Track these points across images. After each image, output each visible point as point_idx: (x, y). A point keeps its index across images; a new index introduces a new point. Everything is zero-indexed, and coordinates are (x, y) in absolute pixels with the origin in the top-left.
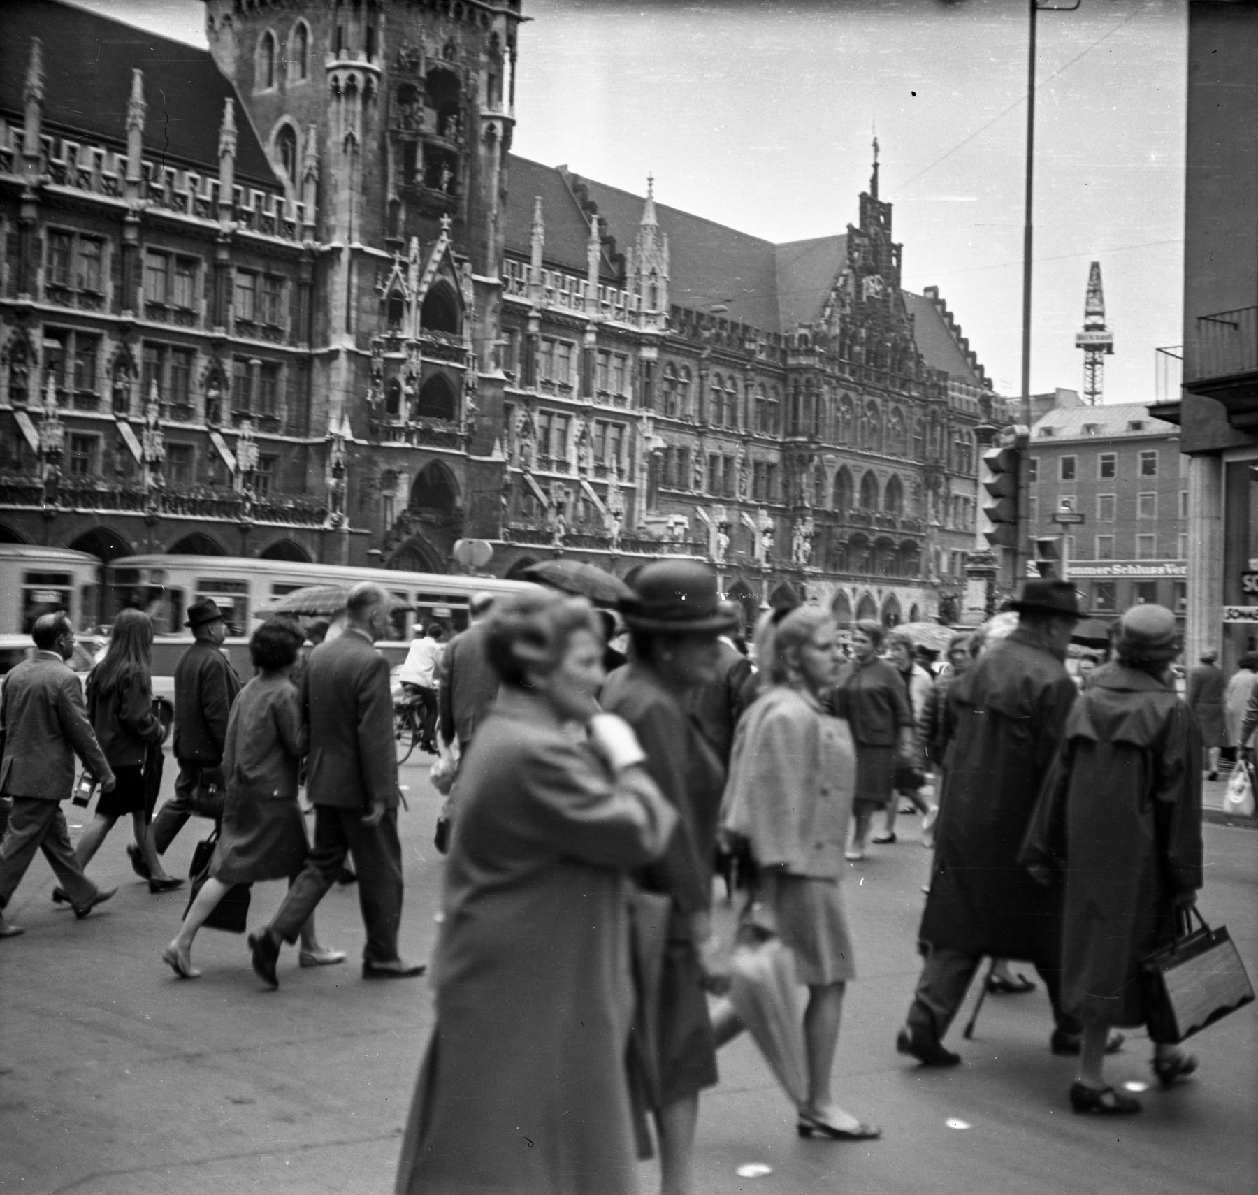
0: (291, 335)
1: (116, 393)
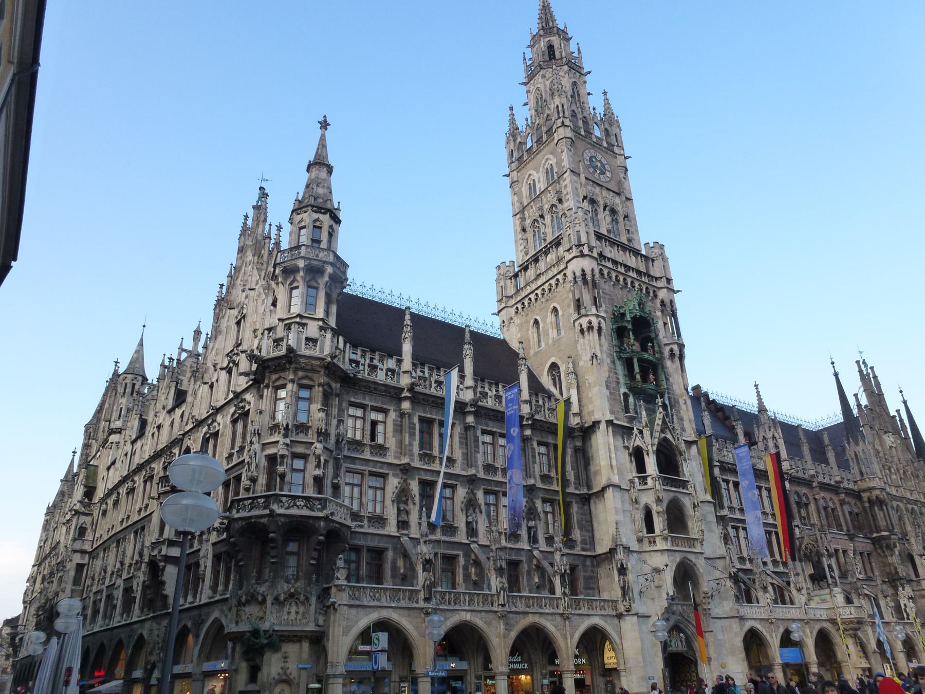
0: (575, 483)
1: (468, 524)
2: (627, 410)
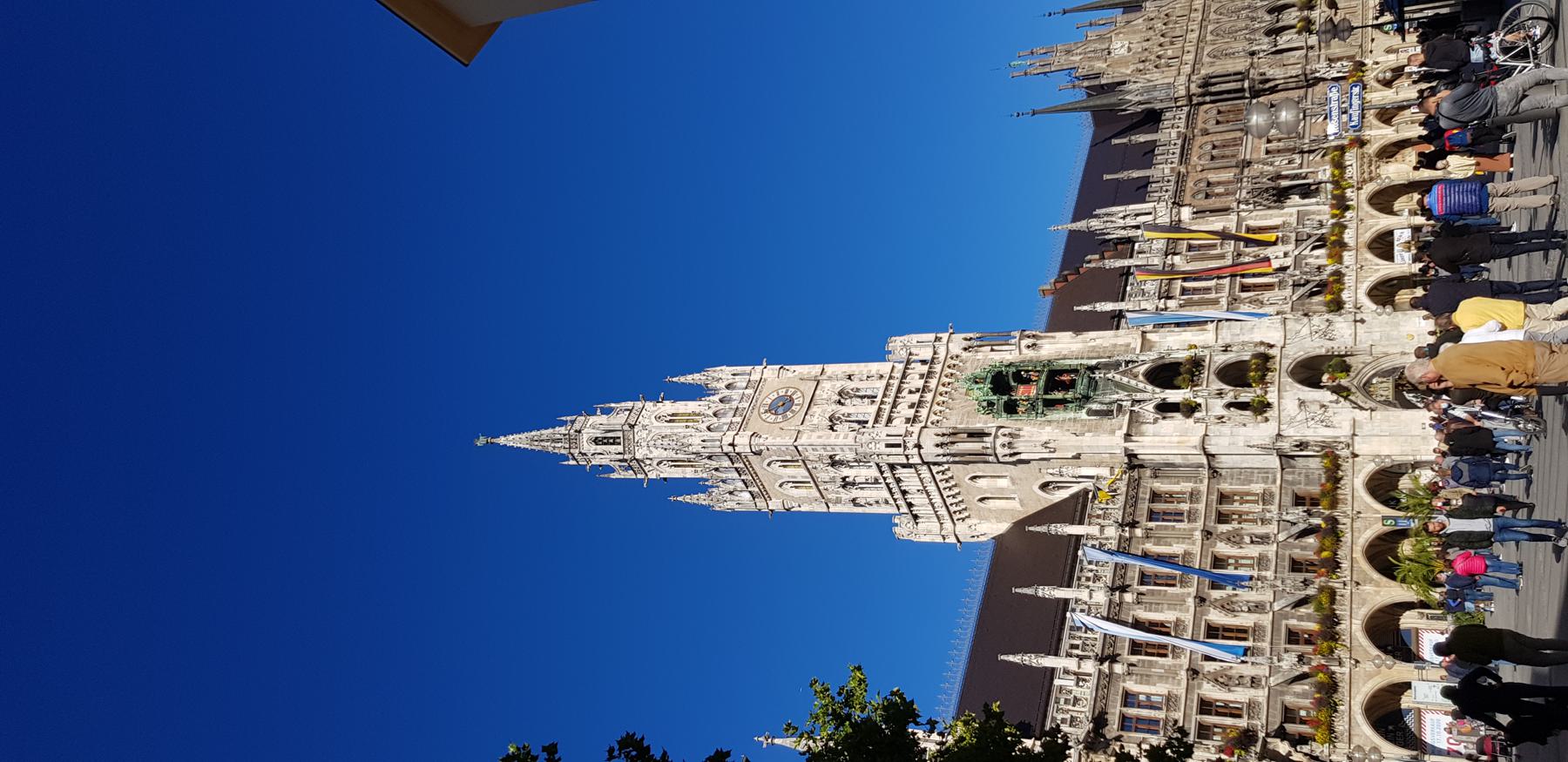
1: (1249, 611)
2: (1108, 413)
